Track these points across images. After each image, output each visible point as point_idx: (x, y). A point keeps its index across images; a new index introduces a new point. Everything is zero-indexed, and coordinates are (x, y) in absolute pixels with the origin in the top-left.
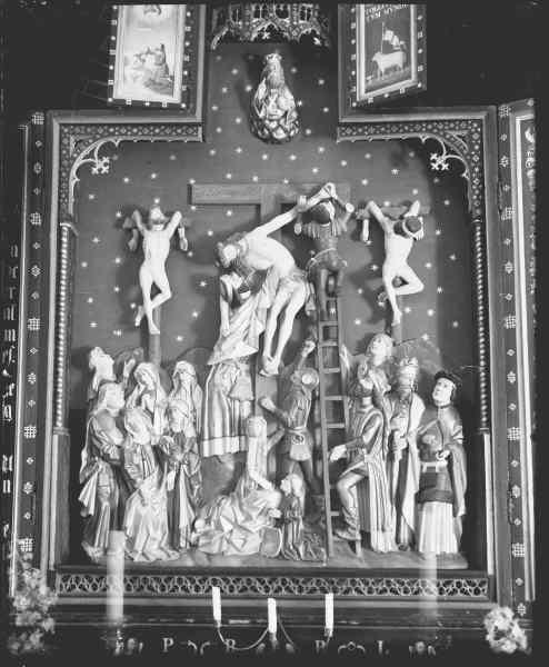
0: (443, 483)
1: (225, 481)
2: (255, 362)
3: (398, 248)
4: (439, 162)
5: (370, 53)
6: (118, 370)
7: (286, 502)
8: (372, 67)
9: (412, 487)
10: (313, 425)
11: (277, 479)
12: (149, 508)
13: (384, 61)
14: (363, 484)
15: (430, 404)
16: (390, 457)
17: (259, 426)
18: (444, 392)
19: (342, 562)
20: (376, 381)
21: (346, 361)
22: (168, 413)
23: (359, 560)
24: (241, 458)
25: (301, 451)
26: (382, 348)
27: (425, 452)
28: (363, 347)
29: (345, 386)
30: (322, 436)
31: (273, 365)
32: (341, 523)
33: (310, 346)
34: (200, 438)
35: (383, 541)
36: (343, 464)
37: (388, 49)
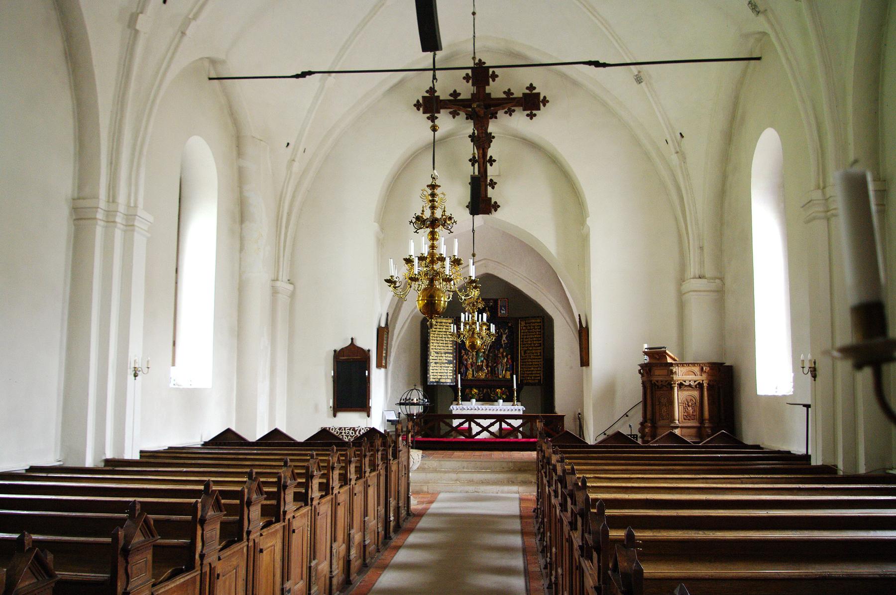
0: (509, 369)
1: (480, 368)
2: (484, 352)
3: (504, 337)
4: (510, 325)
5: (500, 310)
6: (465, 353)
7: (488, 371)
8: (500, 312)
9: (504, 369)
10: (492, 361)
11: (487, 369)
12: (470, 371)
13: (502, 312)
14: (498, 369)
15: (507, 358)
16: (502, 366)
17: (485, 361)
18: (509, 357)
19: (495, 378)
20: (500, 355)
21: (496, 352)
22: (472, 359)
23: (498, 379)
24: (482, 365)
25: (490, 364)
26: (501, 350)
27: (507, 365)
28: (499, 350)
29: (496, 356)
30: (493, 363)
31: (487, 352)
32: (495, 374)
33: (492, 350)
34: (477, 363)
35: (500, 377)
36: (496, 366)
37: (503, 310)
